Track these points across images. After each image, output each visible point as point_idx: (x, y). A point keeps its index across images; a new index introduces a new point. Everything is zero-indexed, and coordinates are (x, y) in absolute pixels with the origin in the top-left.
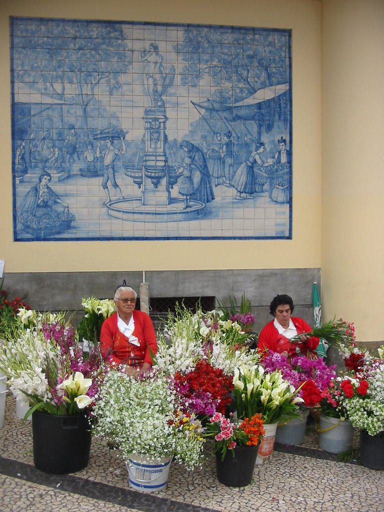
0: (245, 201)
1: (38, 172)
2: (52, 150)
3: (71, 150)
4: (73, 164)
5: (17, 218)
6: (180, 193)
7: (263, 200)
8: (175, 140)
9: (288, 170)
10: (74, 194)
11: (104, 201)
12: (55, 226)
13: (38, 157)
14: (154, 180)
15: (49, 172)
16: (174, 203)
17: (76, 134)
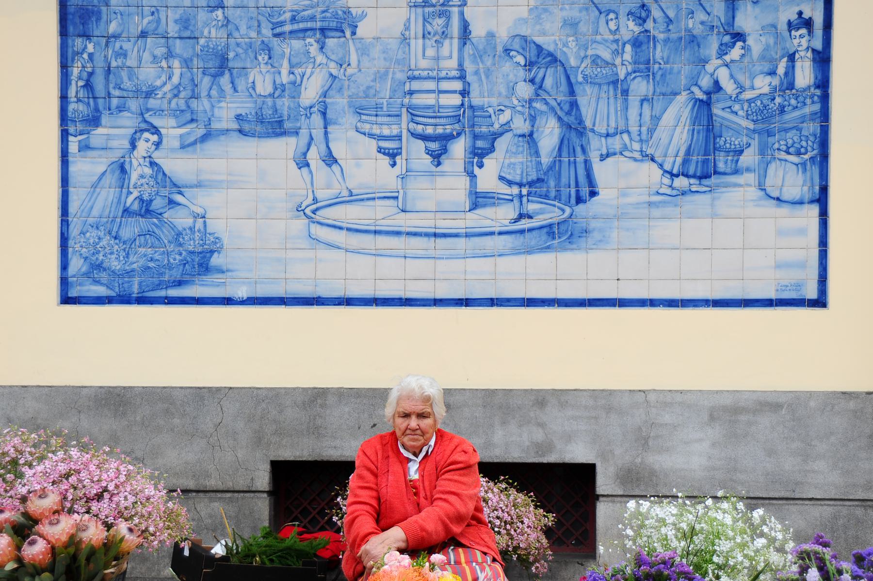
0: (688, 198)
1: (128, 123)
2: (164, 64)
3: (212, 64)
4: (219, 102)
5: (71, 243)
6: (501, 178)
7: (738, 195)
8: (491, 35)
9: (817, 107)
10: (221, 181)
11: (298, 200)
12: (170, 267)
13: (127, 84)
14: (434, 146)
15: (156, 122)
16: (484, 206)
17: (227, 21)
